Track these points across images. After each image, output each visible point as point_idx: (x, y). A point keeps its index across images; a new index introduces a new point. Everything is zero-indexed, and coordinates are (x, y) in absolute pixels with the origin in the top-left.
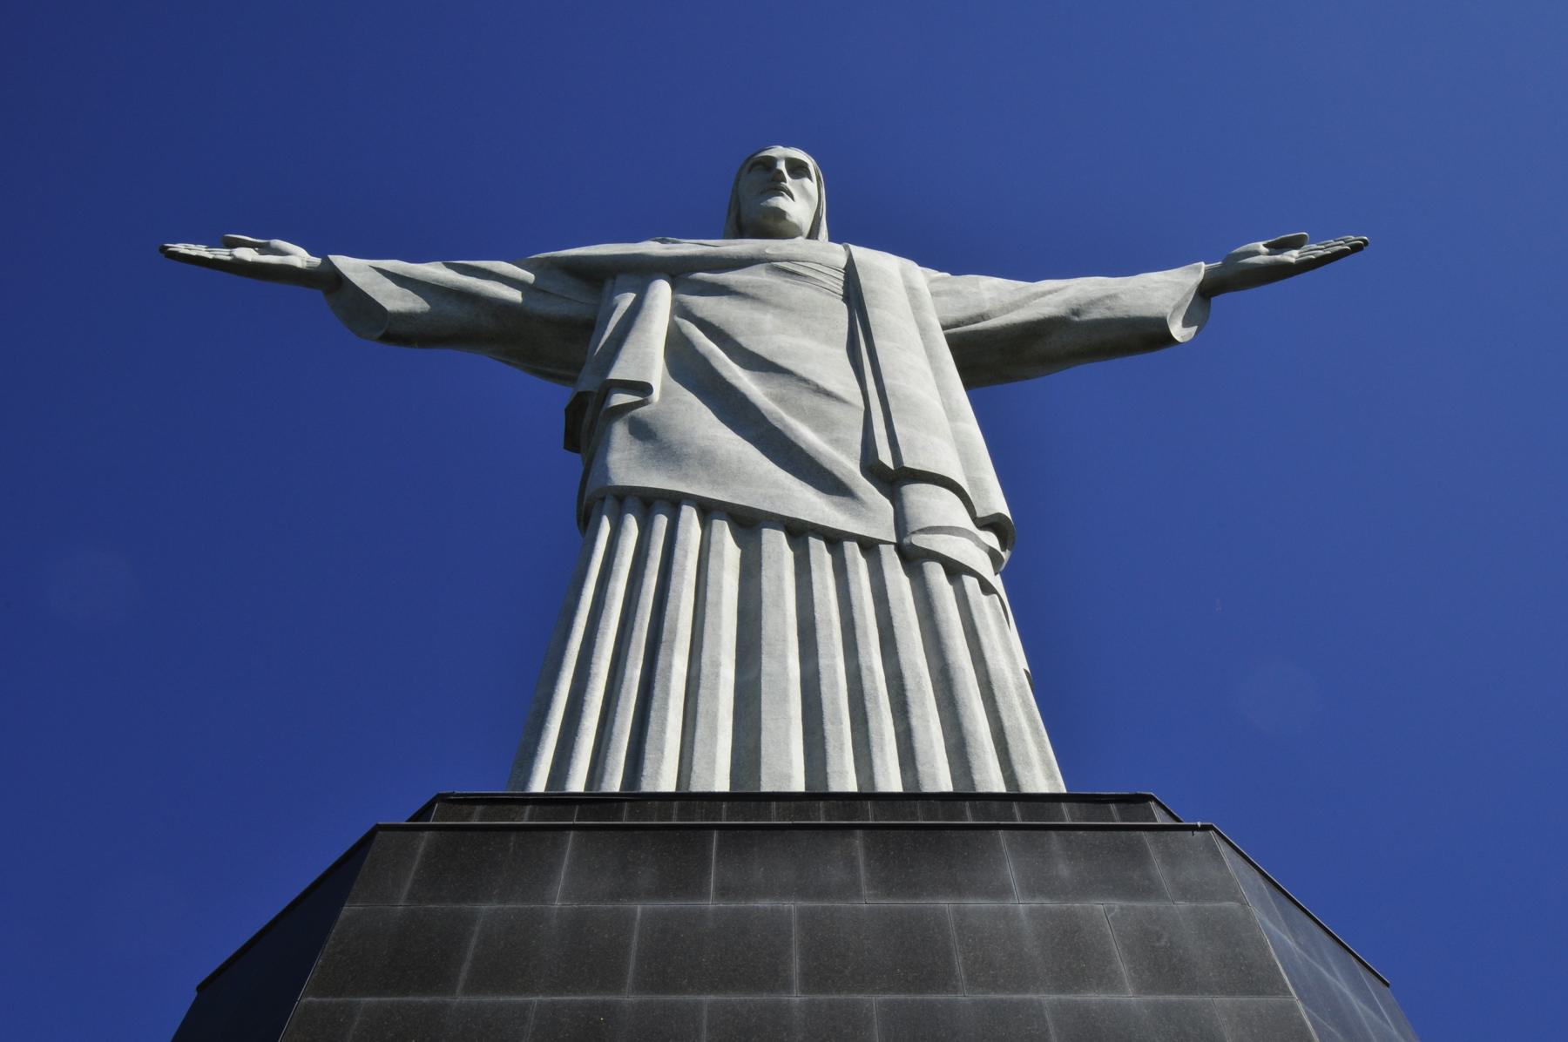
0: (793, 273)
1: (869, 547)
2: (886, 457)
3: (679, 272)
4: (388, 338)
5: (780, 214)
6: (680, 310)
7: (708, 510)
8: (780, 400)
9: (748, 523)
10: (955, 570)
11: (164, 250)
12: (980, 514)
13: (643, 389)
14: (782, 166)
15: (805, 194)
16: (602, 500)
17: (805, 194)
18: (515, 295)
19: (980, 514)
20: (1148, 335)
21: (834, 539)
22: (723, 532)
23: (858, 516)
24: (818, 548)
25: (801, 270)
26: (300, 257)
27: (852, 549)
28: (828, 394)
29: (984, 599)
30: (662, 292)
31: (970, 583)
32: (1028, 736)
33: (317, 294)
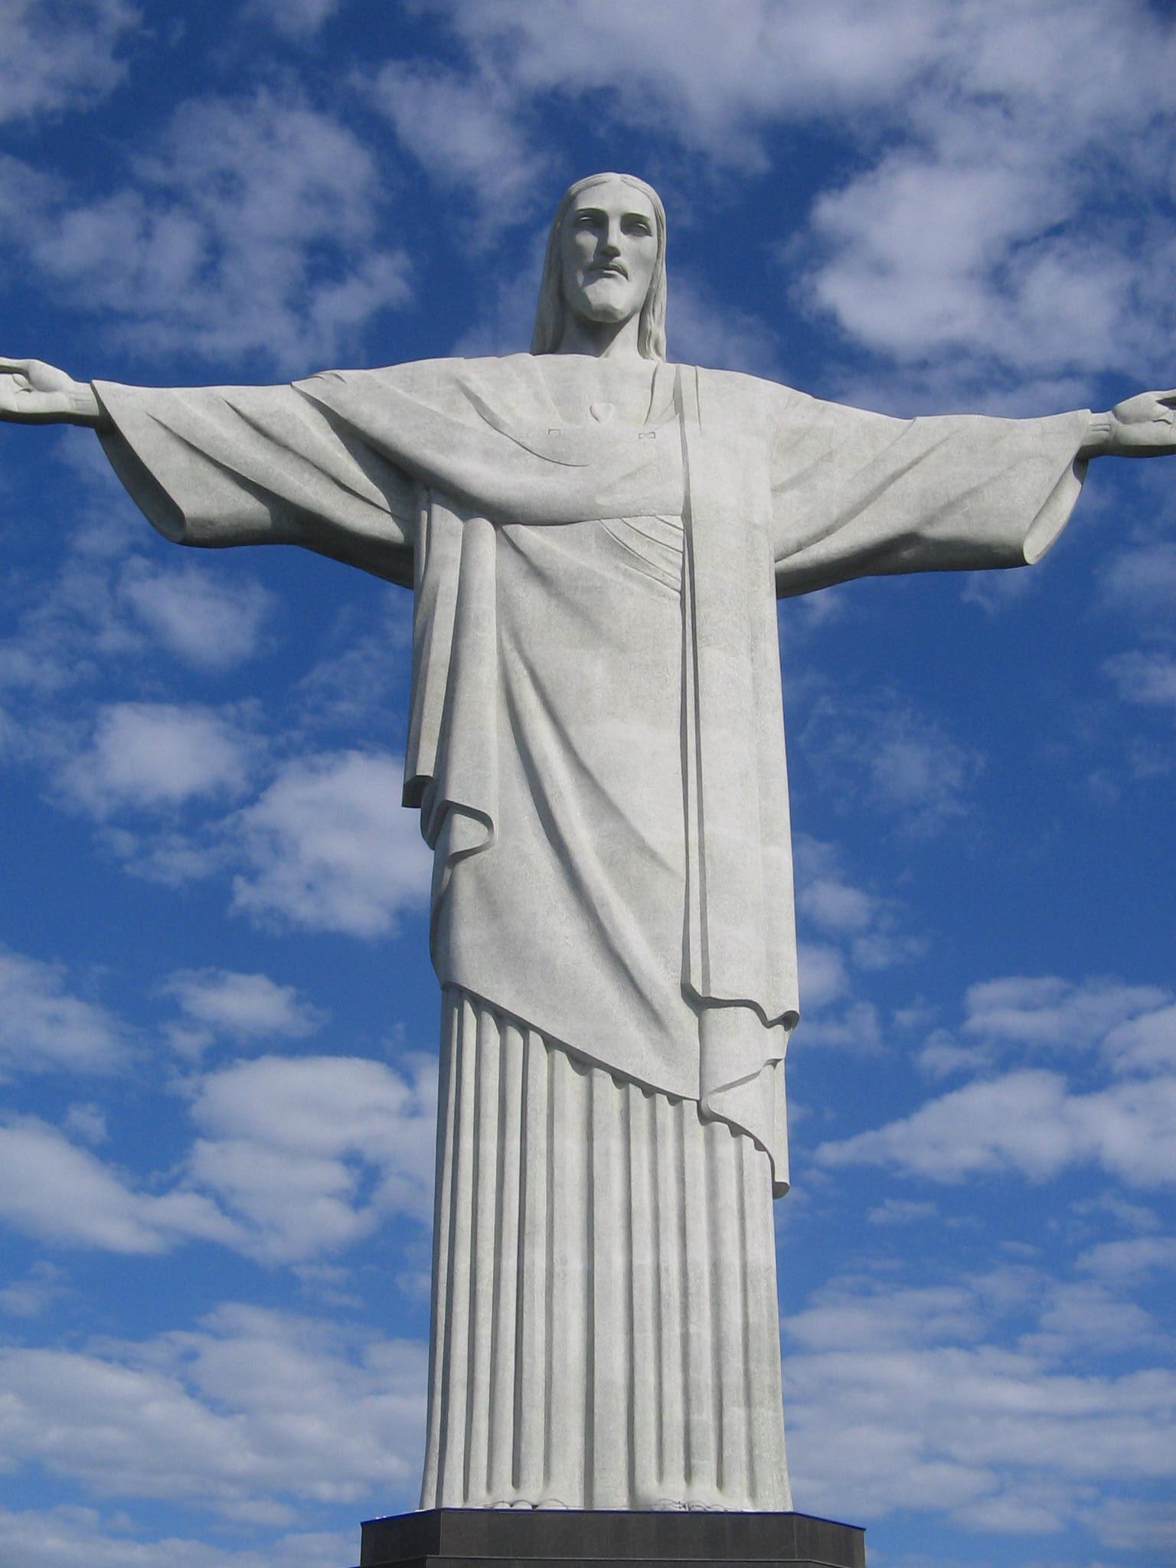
0: (624, 551)
1: (675, 1100)
2: (697, 985)
3: (501, 516)
5: (607, 312)
6: (505, 606)
7: (551, 1043)
8: (610, 862)
9: (583, 1062)
10: (737, 1130)
12: (771, 1017)
16: (455, 994)
17: (641, 260)
19: (771, 1017)
21: (649, 1091)
25: (632, 543)
29: (759, 1155)
31: (748, 1142)
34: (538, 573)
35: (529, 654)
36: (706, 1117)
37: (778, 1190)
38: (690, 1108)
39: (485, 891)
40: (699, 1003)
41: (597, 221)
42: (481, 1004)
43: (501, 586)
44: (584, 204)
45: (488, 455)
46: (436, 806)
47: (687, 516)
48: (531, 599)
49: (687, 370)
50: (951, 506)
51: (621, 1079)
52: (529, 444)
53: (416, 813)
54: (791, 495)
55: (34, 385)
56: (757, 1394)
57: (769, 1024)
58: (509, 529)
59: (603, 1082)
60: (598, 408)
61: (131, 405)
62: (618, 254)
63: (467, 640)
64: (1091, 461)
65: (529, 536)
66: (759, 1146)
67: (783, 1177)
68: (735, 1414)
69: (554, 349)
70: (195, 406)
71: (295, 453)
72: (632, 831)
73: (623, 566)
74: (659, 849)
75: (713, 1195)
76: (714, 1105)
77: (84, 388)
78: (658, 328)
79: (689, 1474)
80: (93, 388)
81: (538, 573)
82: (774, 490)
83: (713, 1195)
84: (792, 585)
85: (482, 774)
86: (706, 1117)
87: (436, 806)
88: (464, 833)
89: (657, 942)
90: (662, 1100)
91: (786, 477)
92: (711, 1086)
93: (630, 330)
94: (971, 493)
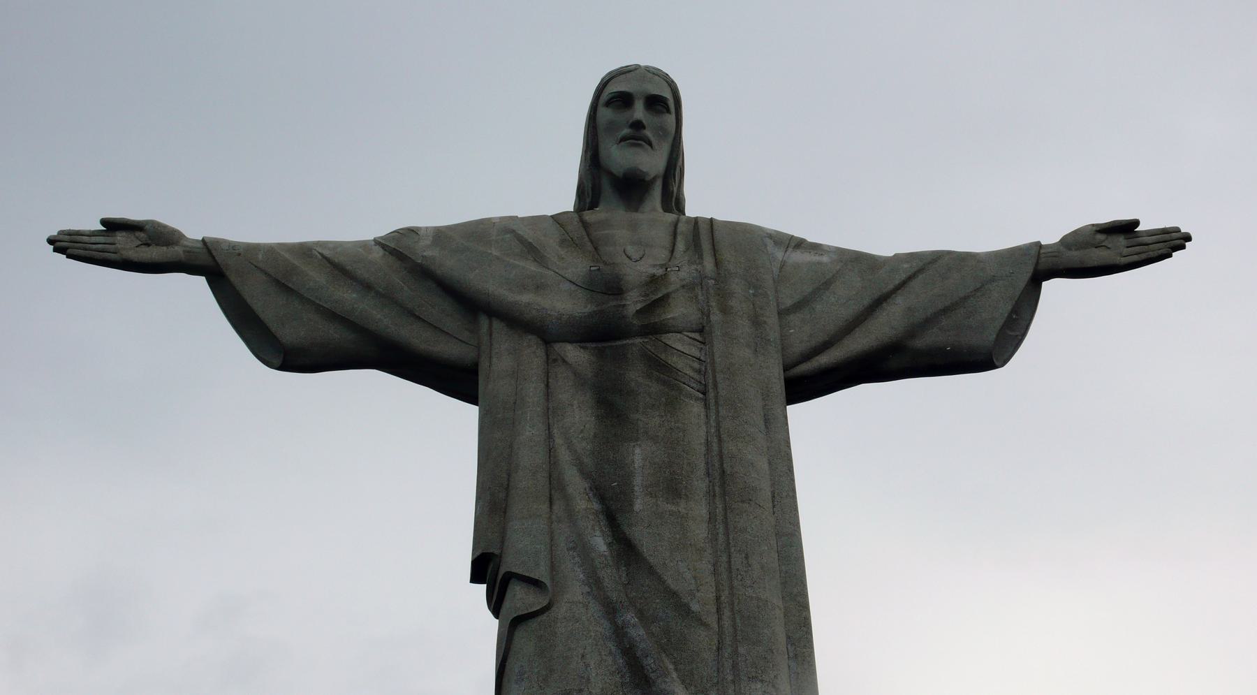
4: (286, 366)
14: (639, 111)
15: (661, 131)
33: (201, 281)
41: (623, 101)
44: (614, 88)
45: (539, 287)
46: (500, 577)
50: (928, 322)
52: (574, 280)
53: (484, 587)
54: (794, 319)
58: (558, 347)
60: (630, 250)
62: (644, 127)
64: (1045, 284)
69: (593, 205)
71: (377, 293)
73: (656, 373)
82: (782, 313)
87: (500, 577)
91: (789, 302)
94: (945, 311)
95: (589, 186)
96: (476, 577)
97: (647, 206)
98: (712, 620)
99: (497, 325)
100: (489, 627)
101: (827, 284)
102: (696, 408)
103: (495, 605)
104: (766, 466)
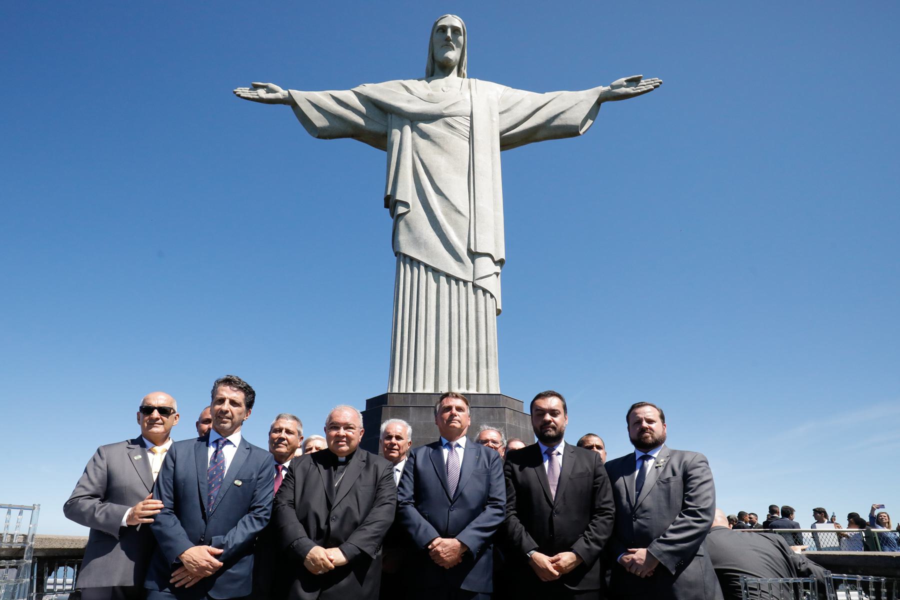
1: (465, 282)
2: (472, 248)
3: (414, 119)
4: (319, 137)
7: (427, 267)
8: (446, 215)
9: (436, 272)
10: (485, 291)
11: (235, 93)
13: (406, 204)
18: (361, 121)
20: (571, 132)
21: (457, 280)
22: (430, 274)
23: (463, 269)
24: (453, 282)
26: (281, 93)
27: (461, 283)
28: (459, 212)
30: (407, 129)
31: (488, 295)
32: (493, 353)
33: (289, 108)
34: (425, 135)
35: (422, 157)
36: (475, 287)
37: (498, 312)
38: (470, 285)
39: (407, 225)
40: (474, 255)
42: (405, 256)
43: (413, 139)
47: (471, 116)
48: (422, 143)
49: (473, 80)
51: (449, 277)
54: (504, 115)
55: (270, 91)
56: (490, 365)
57: (496, 263)
59: (443, 279)
61: (300, 96)
63: (402, 155)
65: (422, 125)
66: (492, 296)
67: (499, 307)
68: (483, 370)
69: (432, 75)
70: (323, 97)
72: (452, 205)
74: (461, 210)
75: (477, 311)
76: (478, 283)
77: (286, 92)
78: (464, 71)
79: (468, 388)
80: (289, 93)
81: (425, 135)
83: (477, 311)
84: (508, 142)
85: (406, 191)
86: (475, 287)
88: (401, 210)
89: (460, 237)
90: (461, 283)
91: (503, 110)
92: (477, 276)
93: (455, 70)
94: (562, 113)
95: (430, 67)
96: (387, 206)
97: (451, 75)
98: (467, 215)
99: (394, 116)
100: (391, 221)
101: (518, 103)
102: (466, 144)
103: (393, 214)
104: (490, 164)
